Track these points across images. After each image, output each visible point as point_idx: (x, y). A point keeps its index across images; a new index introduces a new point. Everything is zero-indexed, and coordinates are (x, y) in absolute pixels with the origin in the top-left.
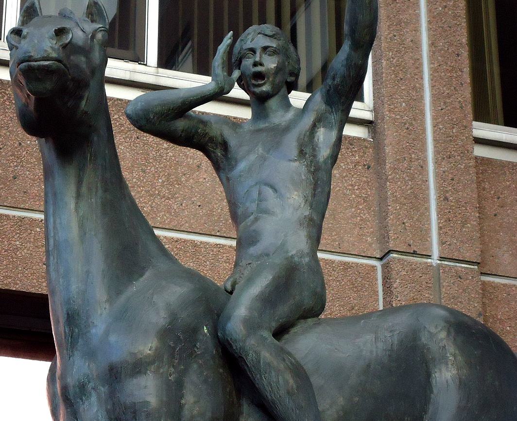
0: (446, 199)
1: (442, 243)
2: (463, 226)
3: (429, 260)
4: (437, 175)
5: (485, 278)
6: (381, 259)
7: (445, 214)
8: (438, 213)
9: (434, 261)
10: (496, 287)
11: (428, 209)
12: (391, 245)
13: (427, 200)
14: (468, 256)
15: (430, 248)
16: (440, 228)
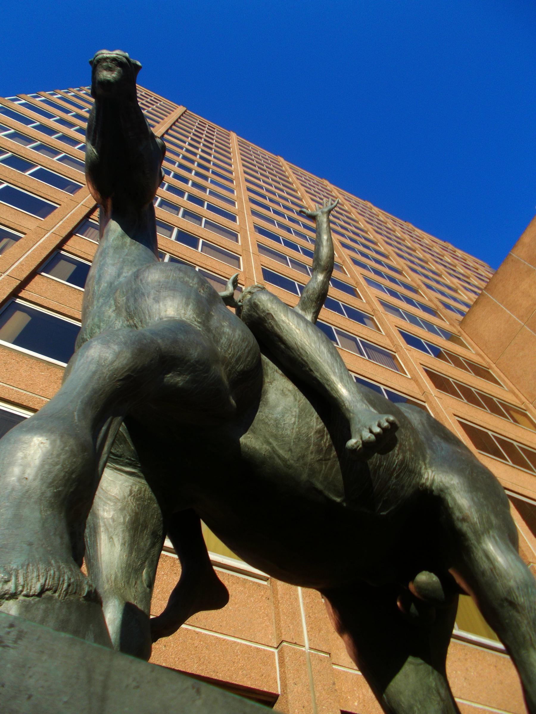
0: (309, 617)
1: (310, 640)
2: (320, 632)
3: (304, 649)
4: (304, 604)
5: (334, 667)
6: (277, 648)
7: (310, 624)
8: (306, 624)
9: (306, 649)
10: (339, 672)
11: (301, 620)
12: (283, 638)
13: (300, 615)
14: (324, 649)
15: (304, 641)
16: (308, 632)
